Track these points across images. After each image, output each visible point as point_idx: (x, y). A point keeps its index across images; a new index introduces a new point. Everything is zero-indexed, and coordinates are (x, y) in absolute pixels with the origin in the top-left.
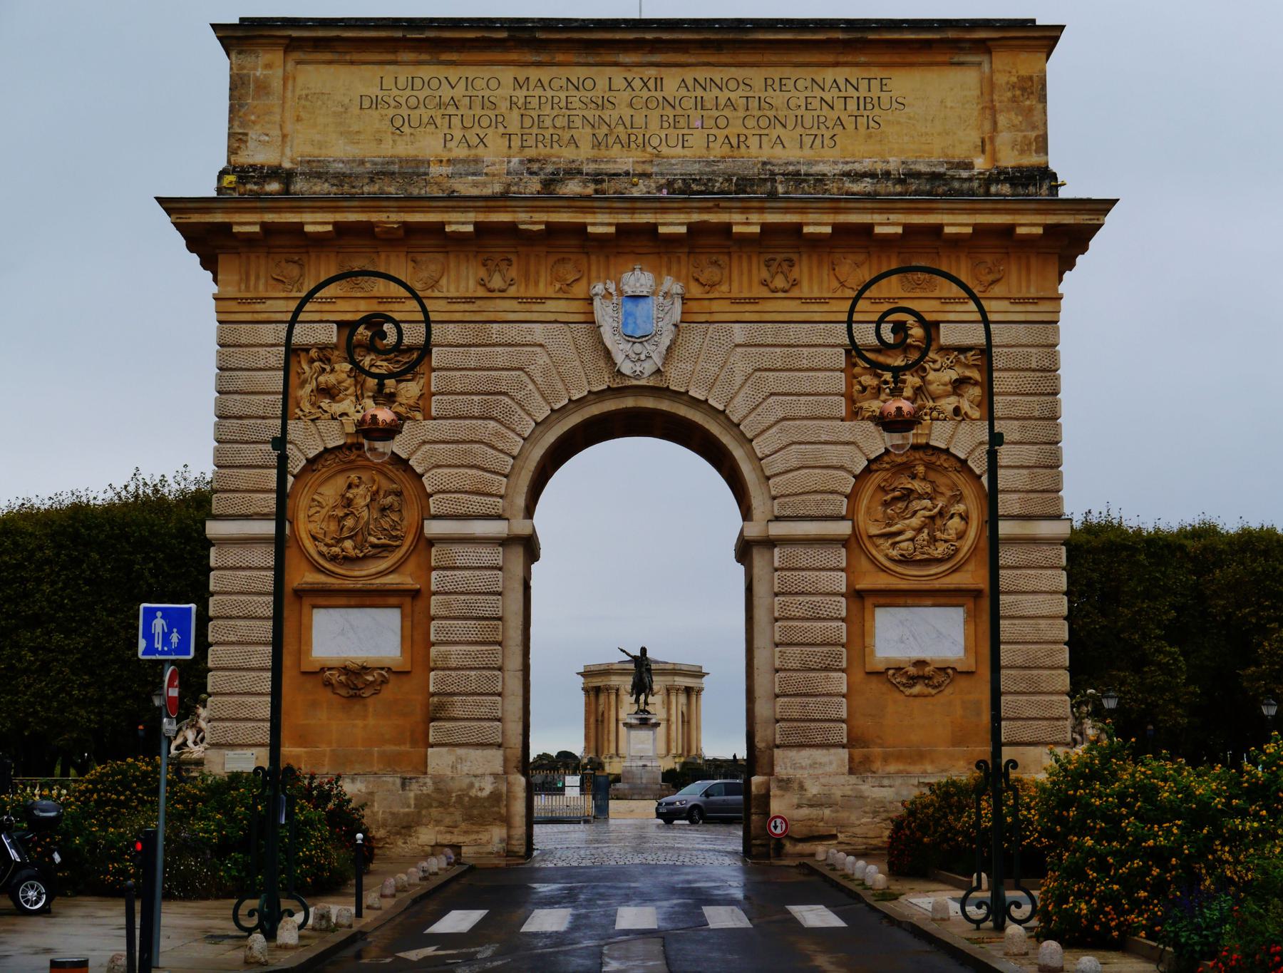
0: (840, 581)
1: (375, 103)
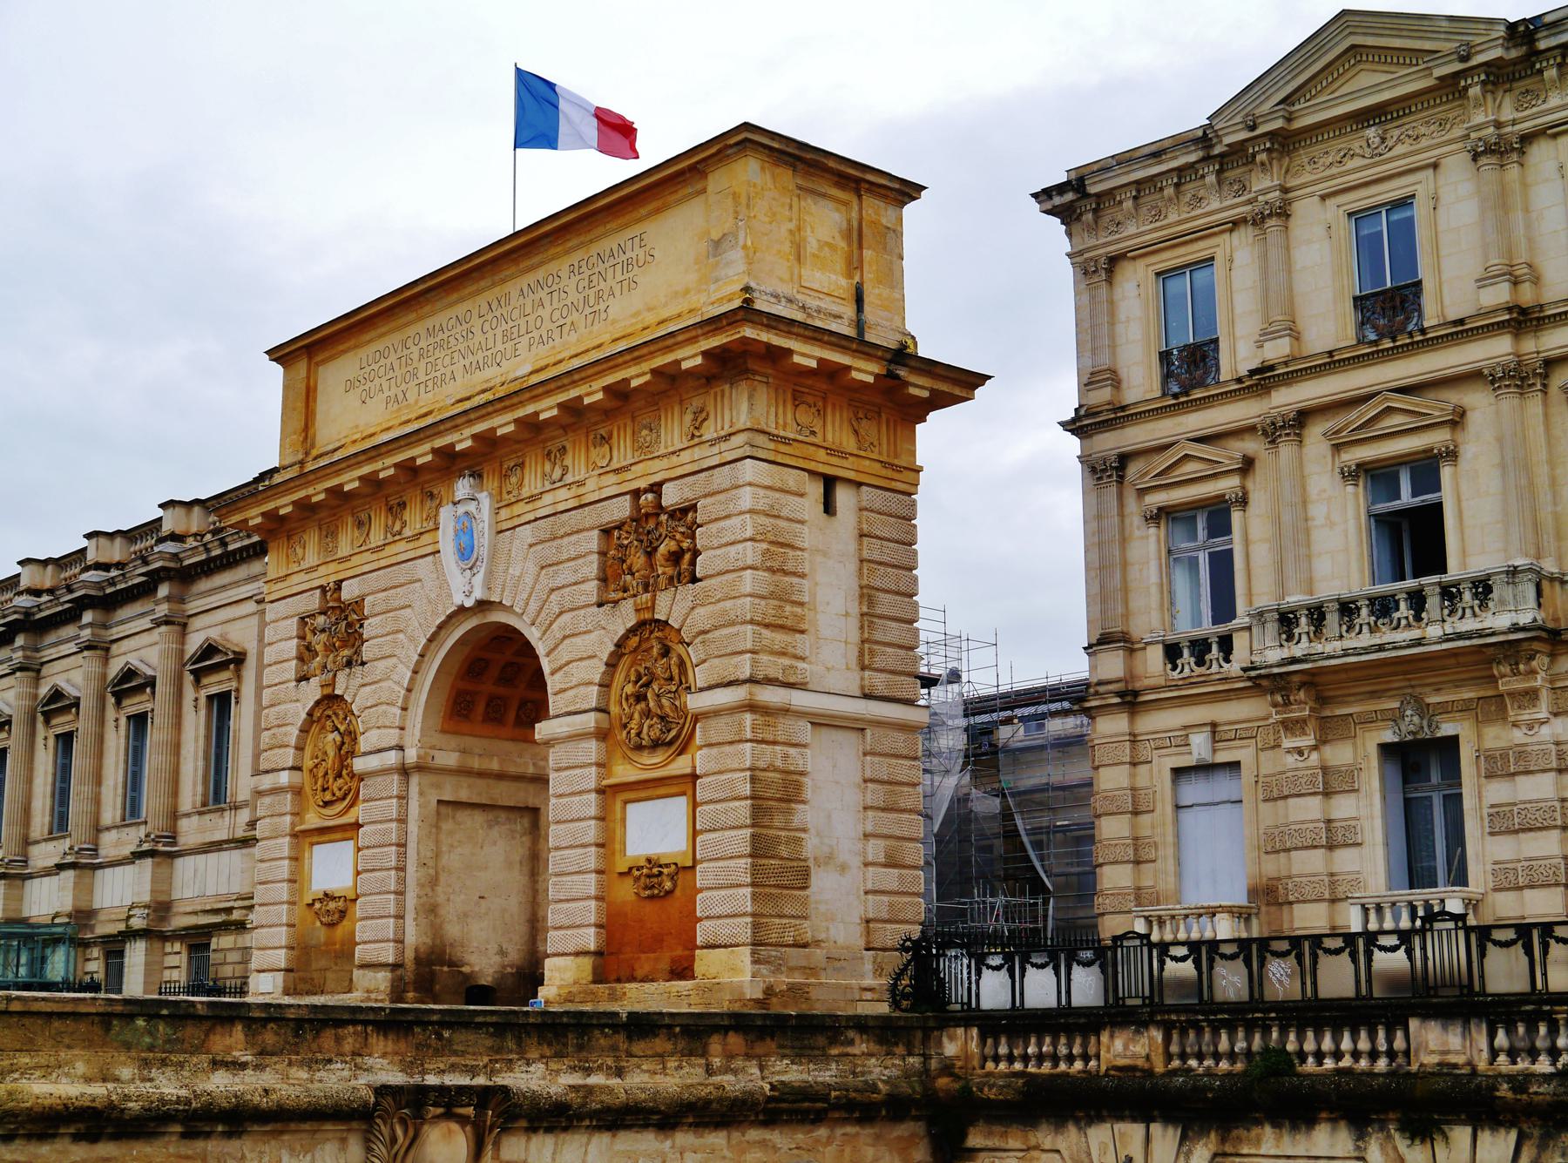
0: (590, 777)
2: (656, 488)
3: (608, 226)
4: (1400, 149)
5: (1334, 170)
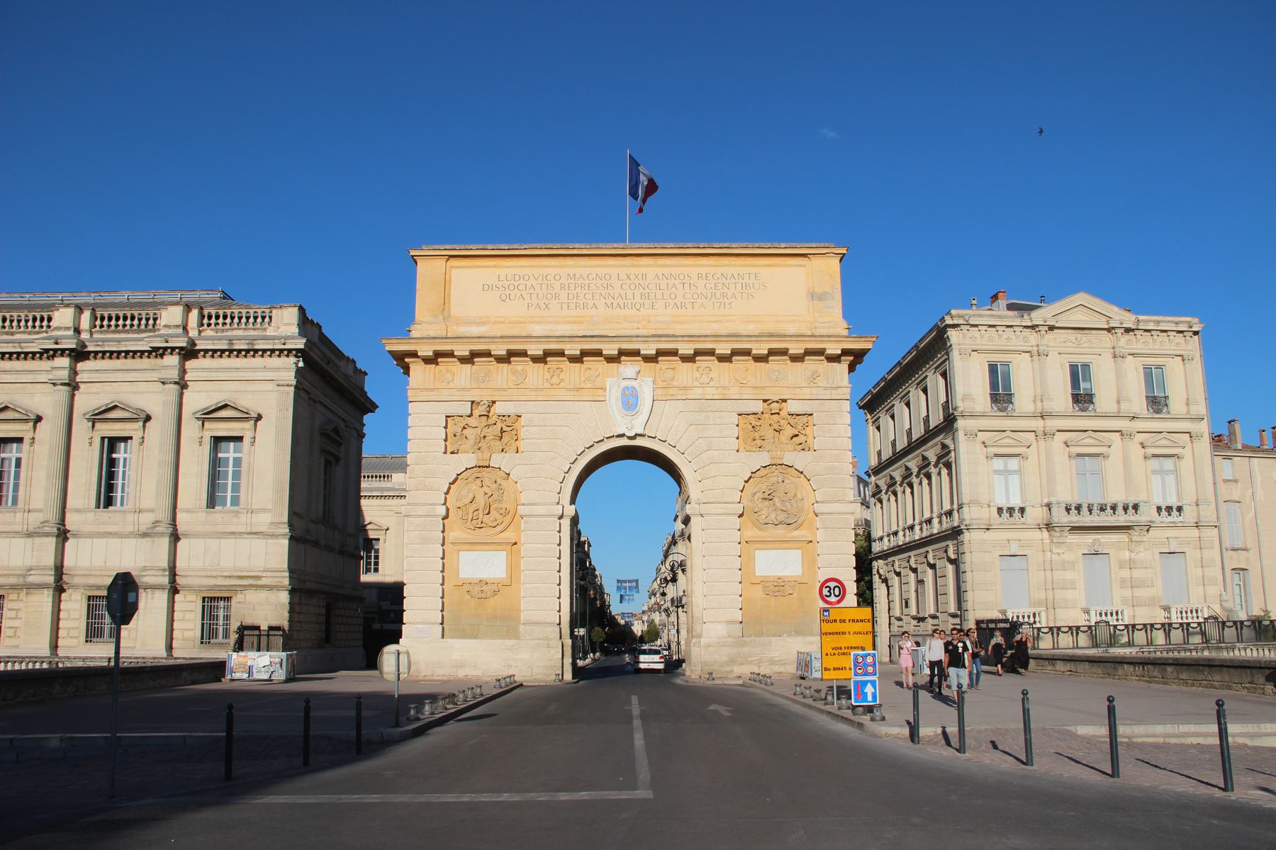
1: (490, 287)
2: (784, 401)
3: (733, 263)
4: (1085, 345)
5: (1063, 345)
